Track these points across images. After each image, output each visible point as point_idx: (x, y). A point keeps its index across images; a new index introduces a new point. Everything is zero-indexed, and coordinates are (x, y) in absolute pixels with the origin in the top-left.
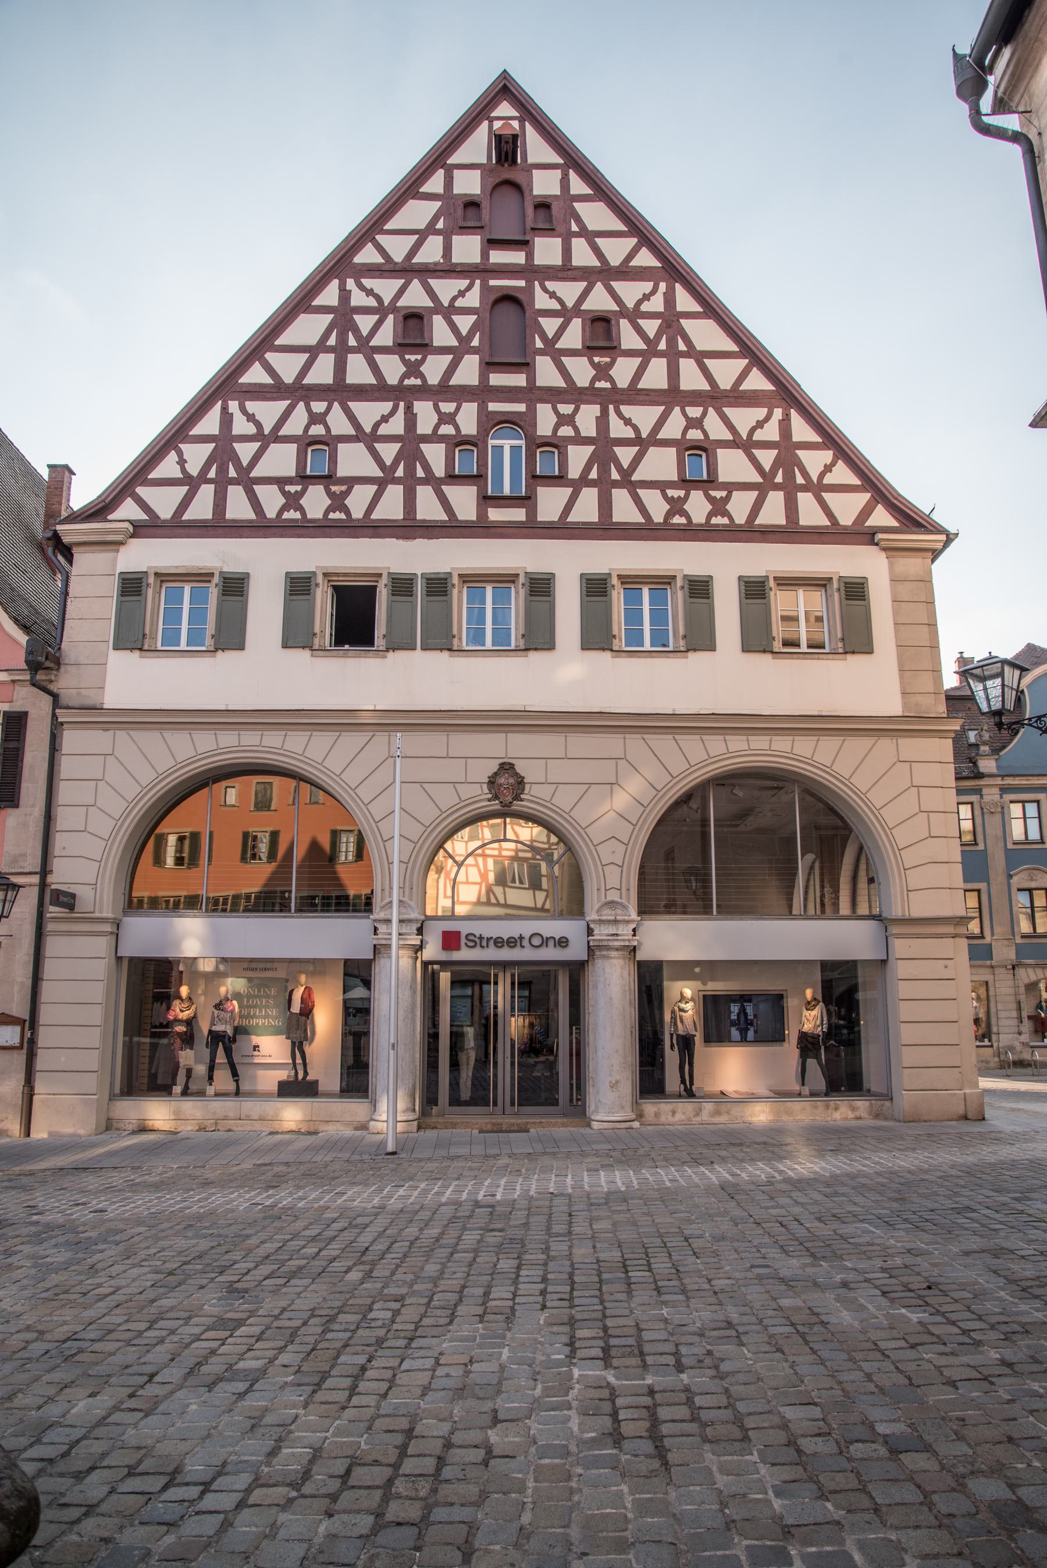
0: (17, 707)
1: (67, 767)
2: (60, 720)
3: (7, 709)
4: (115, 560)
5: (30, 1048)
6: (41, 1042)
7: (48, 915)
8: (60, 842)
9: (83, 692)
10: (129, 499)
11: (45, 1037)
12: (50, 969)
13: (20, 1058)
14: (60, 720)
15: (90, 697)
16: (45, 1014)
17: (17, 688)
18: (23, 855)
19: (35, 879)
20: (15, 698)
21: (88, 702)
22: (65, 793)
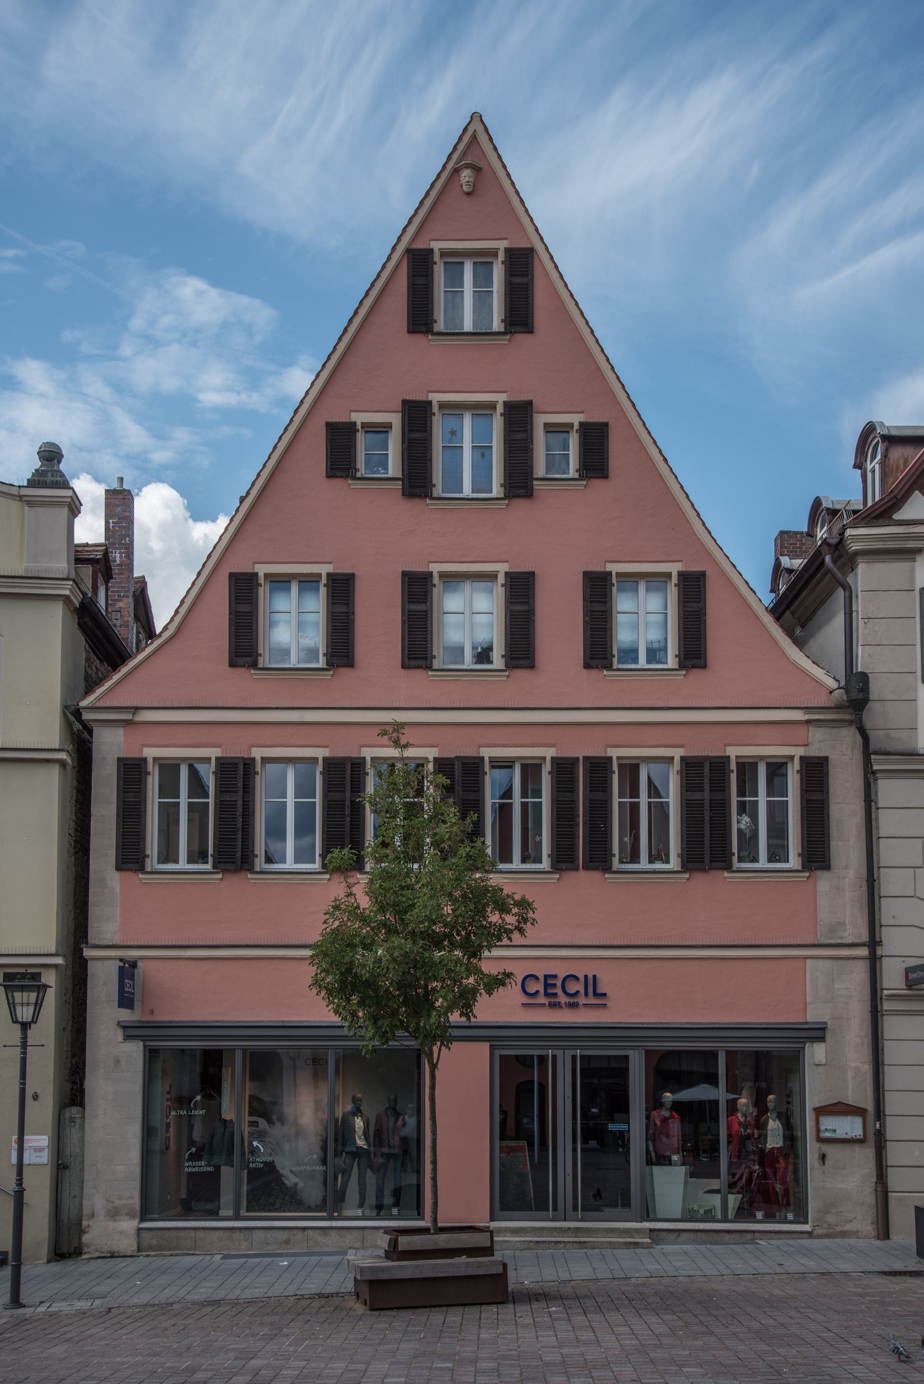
0: (814, 751)
1: (886, 822)
2: (875, 767)
3: (802, 754)
4: (912, 571)
5: (880, 1142)
6: (890, 1135)
7: (885, 992)
8: (888, 910)
9: (893, 733)
10: (917, 492)
11: (894, 1128)
12: (890, 1053)
13: (868, 1152)
14: (875, 767)
15: (901, 741)
16: (892, 1104)
17: (811, 729)
18: (842, 924)
19: (864, 952)
20: (810, 741)
21: (899, 747)
22: (887, 852)
